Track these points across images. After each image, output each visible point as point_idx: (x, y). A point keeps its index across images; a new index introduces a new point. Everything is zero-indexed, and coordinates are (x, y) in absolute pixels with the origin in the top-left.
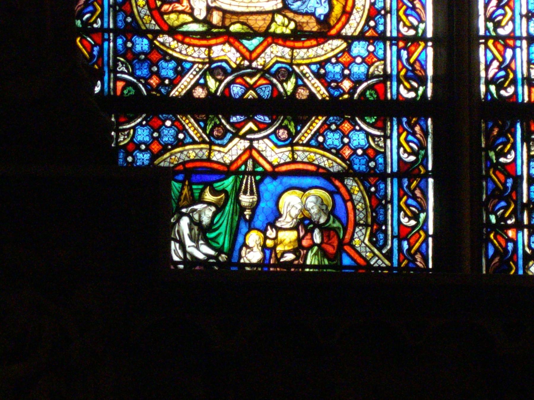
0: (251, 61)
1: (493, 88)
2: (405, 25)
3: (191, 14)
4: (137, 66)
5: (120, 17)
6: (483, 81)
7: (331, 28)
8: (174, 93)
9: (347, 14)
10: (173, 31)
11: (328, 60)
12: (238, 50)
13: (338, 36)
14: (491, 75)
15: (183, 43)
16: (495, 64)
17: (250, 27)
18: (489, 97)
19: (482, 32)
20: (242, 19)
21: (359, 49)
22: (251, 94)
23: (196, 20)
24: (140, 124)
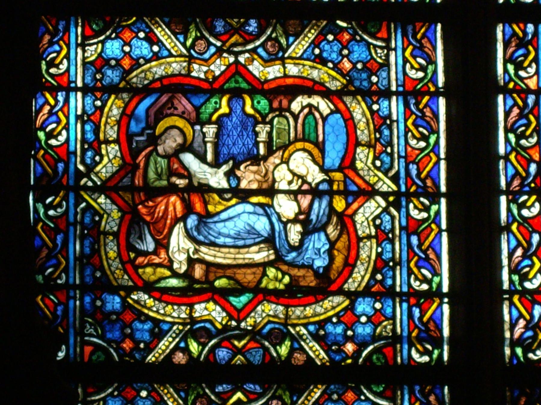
0: (239, 322)
1: (519, 351)
2: (412, 67)
3: (170, 267)
4: (108, 328)
5: (88, 272)
6: (507, 342)
7: (331, 282)
8: (151, 358)
9: (350, 265)
10: (149, 288)
11: (329, 320)
12: (224, 309)
13: (340, 292)
14: (517, 335)
15: (160, 301)
16: (522, 323)
17: (237, 281)
18: (515, 362)
19: (506, 286)
20: (229, 272)
21: (364, 306)
22: (239, 359)
23: (175, 275)
24: (111, 395)
